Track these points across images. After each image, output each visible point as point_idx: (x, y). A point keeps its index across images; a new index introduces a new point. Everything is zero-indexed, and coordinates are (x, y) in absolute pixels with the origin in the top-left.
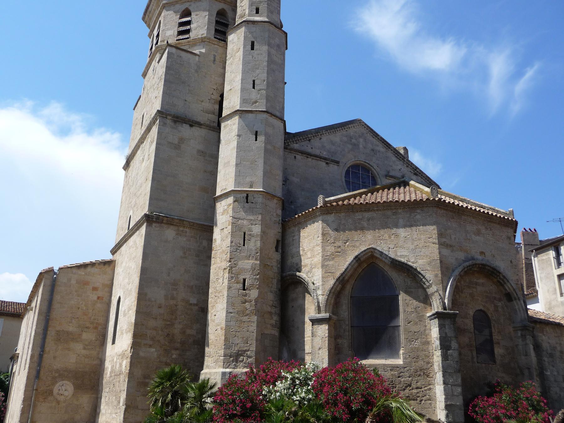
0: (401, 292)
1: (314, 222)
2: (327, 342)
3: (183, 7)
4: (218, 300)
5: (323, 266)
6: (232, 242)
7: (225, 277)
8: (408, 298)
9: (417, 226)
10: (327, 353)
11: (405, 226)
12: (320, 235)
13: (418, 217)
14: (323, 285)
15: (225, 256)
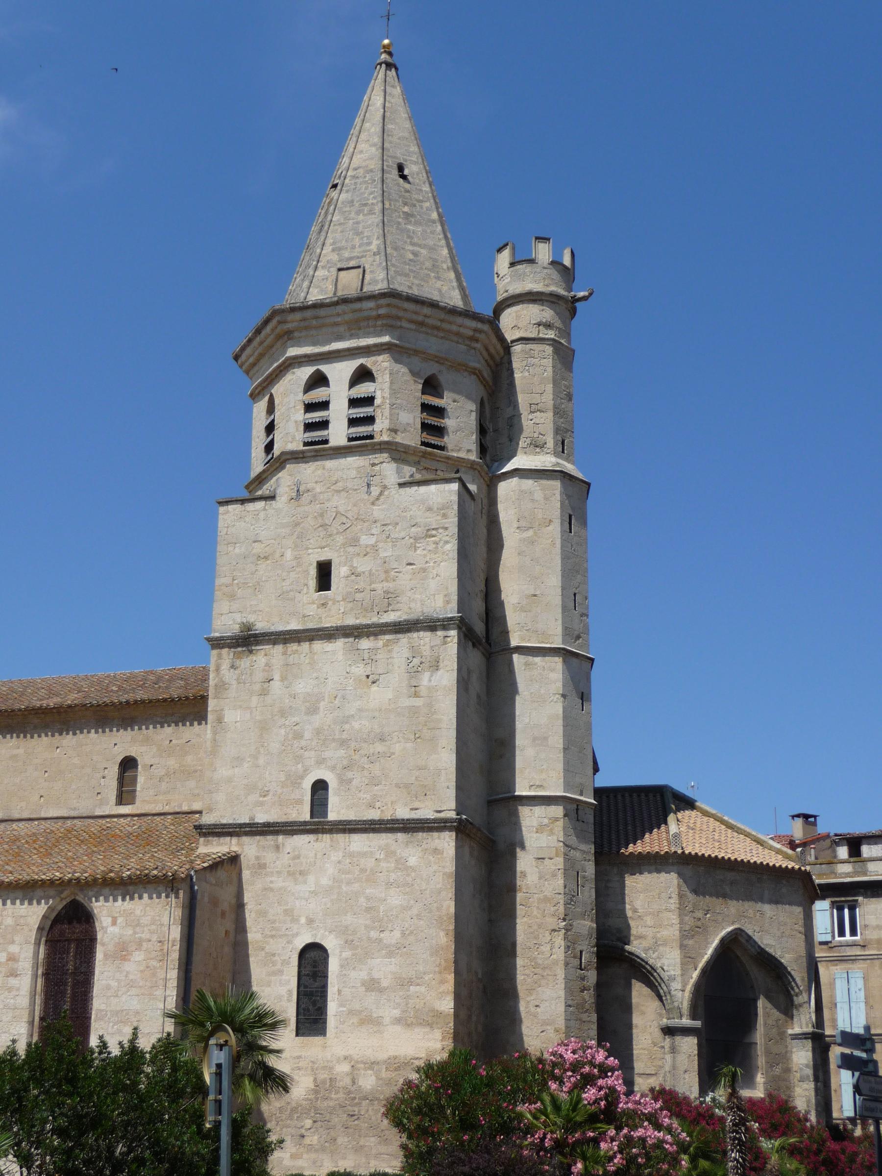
0: (762, 996)
1: (659, 871)
2: (696, 1063)
3: (431, 369)
4: (543, 982)
5: (682, 947)
6: (565, 887)
7: (557, 945)
8: (769, 1005)
9: (783, 903)
10: (697, 1079)
11: (771, 902)
12: (675, 896)
13: (784, 890)
14: (682, 975)
15: (553, 909)
